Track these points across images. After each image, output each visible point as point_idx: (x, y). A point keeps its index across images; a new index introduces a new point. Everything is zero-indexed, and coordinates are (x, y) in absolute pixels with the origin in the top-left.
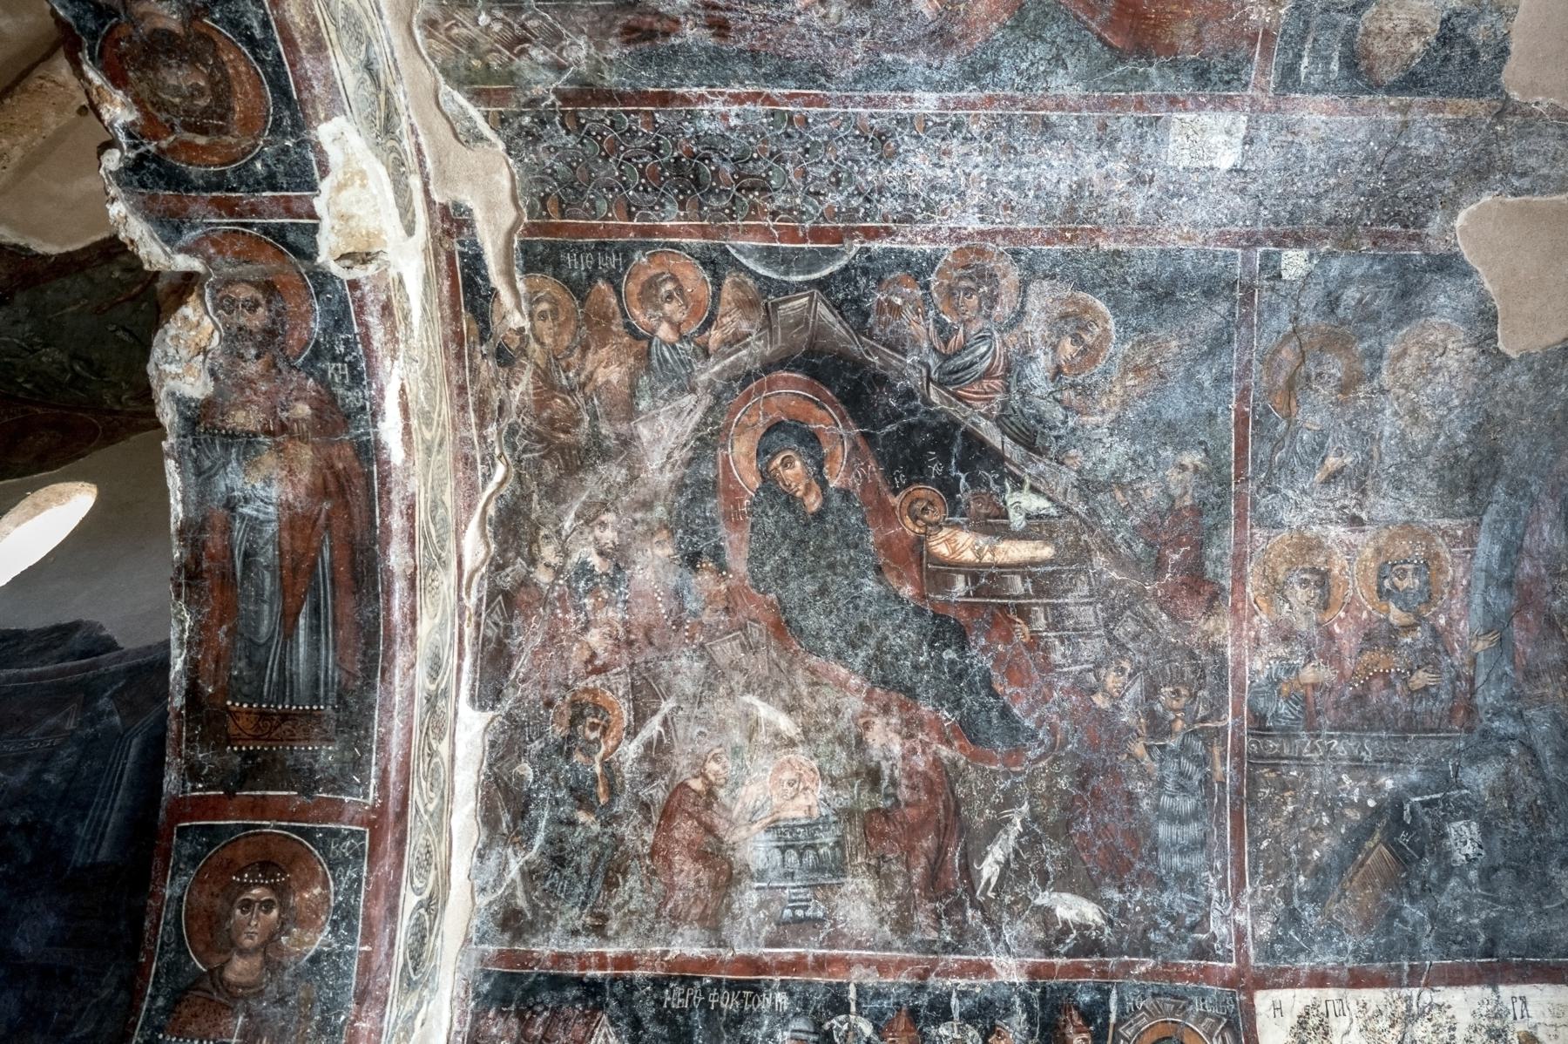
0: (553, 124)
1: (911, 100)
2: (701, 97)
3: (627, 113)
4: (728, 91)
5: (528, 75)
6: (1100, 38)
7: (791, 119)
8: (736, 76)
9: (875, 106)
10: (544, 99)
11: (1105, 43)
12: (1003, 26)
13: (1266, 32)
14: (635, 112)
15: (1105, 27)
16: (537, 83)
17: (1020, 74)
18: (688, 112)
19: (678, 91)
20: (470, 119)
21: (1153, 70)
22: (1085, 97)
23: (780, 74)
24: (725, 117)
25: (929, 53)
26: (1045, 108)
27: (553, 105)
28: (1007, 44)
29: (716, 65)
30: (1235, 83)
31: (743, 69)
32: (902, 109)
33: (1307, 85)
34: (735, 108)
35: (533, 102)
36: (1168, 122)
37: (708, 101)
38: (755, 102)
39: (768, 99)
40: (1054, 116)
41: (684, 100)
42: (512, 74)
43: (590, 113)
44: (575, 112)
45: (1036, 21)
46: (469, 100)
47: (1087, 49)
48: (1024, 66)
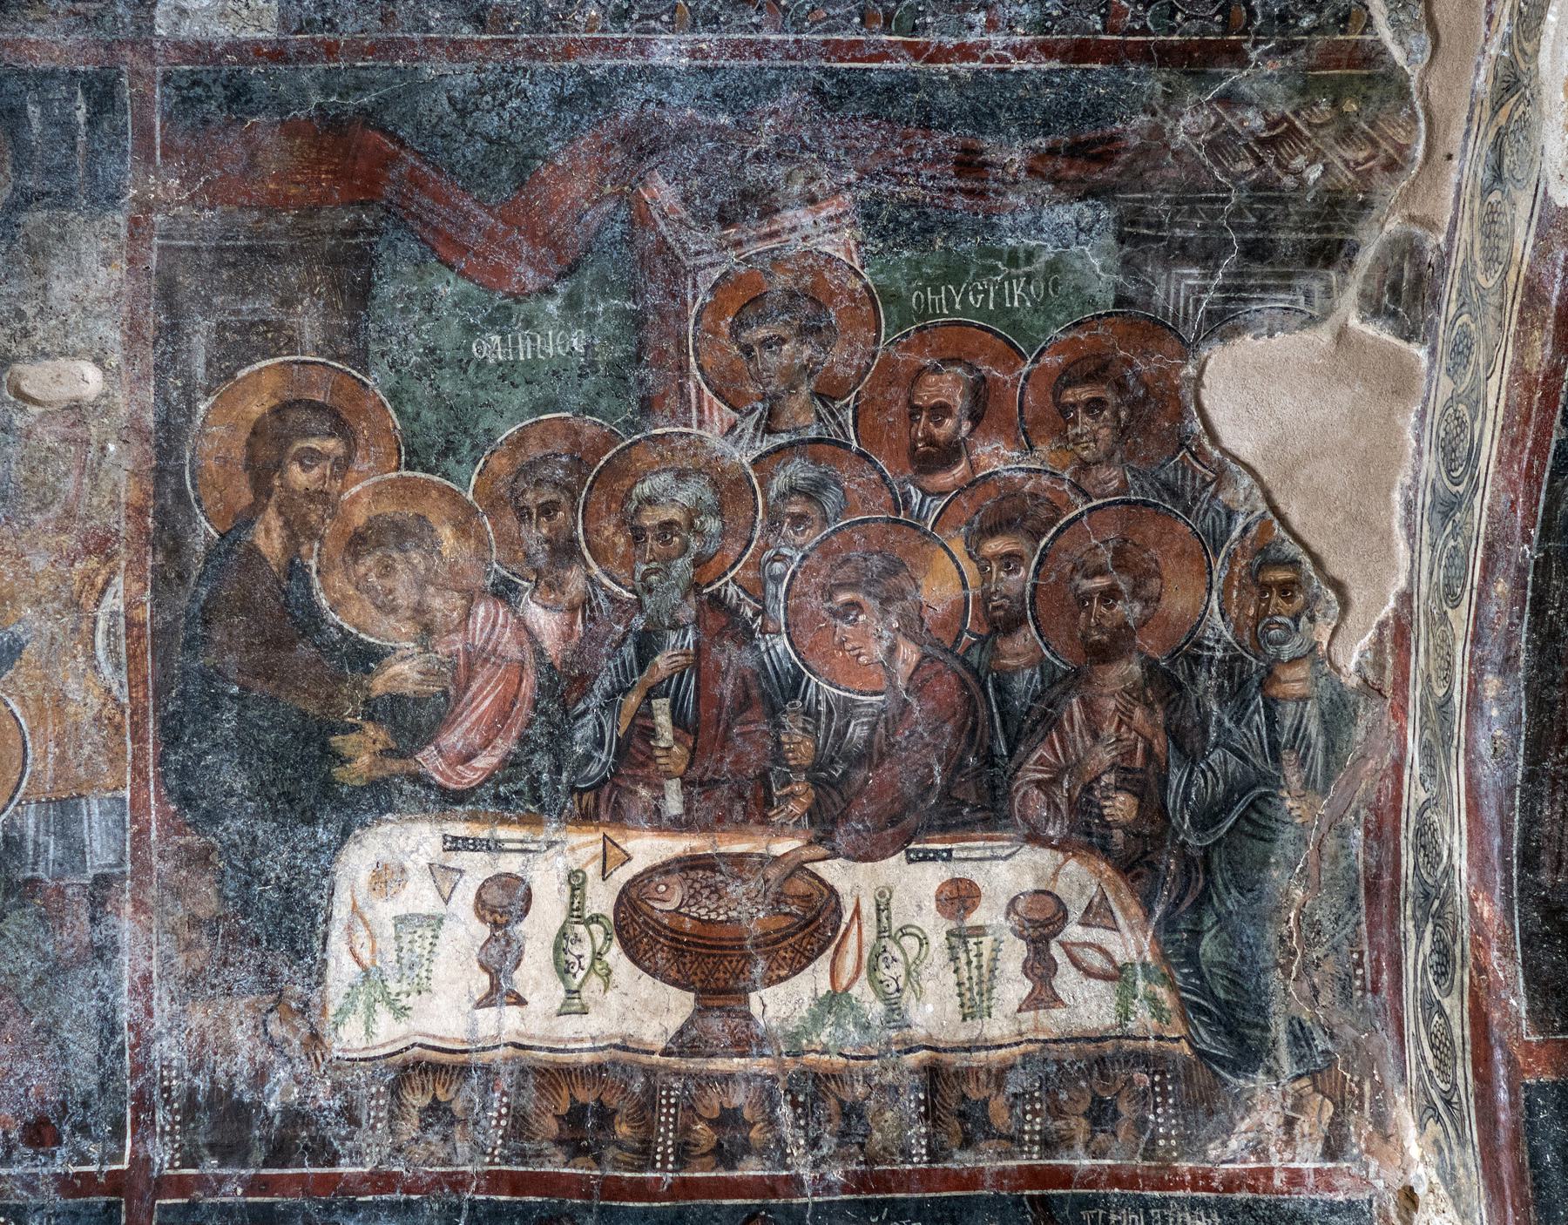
0: (1266, 16)
1: (693, 54)
2: (1021, 53)
3: (1145, 30)
4: (978, 65)
5: (1278, 90)
6: (401, 143)
7: (888, 22)
8: (961, 88)
9: (751, 43)
10: (1267, 53)
11: (392, 136)
12: (549, 160)
13: (149, 158)
14: (1133, 32)
15: (394, 157)
16: (1271, 77)
17: (521, 93)
18: (1049, 31)
19: (1056, 64)
20: (1395, 24)
21: (316, 99)
22: (418, 59)
23: (890, 91)
24: (991, 25)
25: (661, 122)
26: (480, 44)
27: (1256, 44)
28: (541, 133)
29: (988, 104)
30: (184, 83)
31: (947, 98)
32: (707, 39)
33: (69, 83)
34: (971, 39)
35: (1283, 50)
36: (284, 23)
37: (1014, 49)
38: (939, 48)
39: (917, 52)
40: (466, 32)
41: (1048, 50)
42: (1303, 92)
43: (1204, 30)
44: (1226, 32)
45: (498, 164)
46: (1385, 51)
47: (418, 127)
48: (515, 103)
